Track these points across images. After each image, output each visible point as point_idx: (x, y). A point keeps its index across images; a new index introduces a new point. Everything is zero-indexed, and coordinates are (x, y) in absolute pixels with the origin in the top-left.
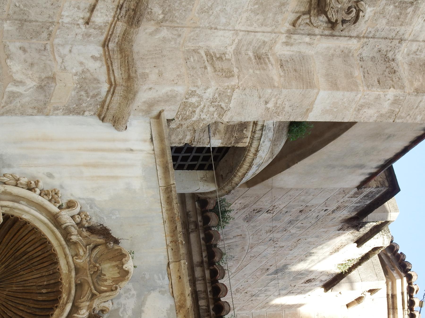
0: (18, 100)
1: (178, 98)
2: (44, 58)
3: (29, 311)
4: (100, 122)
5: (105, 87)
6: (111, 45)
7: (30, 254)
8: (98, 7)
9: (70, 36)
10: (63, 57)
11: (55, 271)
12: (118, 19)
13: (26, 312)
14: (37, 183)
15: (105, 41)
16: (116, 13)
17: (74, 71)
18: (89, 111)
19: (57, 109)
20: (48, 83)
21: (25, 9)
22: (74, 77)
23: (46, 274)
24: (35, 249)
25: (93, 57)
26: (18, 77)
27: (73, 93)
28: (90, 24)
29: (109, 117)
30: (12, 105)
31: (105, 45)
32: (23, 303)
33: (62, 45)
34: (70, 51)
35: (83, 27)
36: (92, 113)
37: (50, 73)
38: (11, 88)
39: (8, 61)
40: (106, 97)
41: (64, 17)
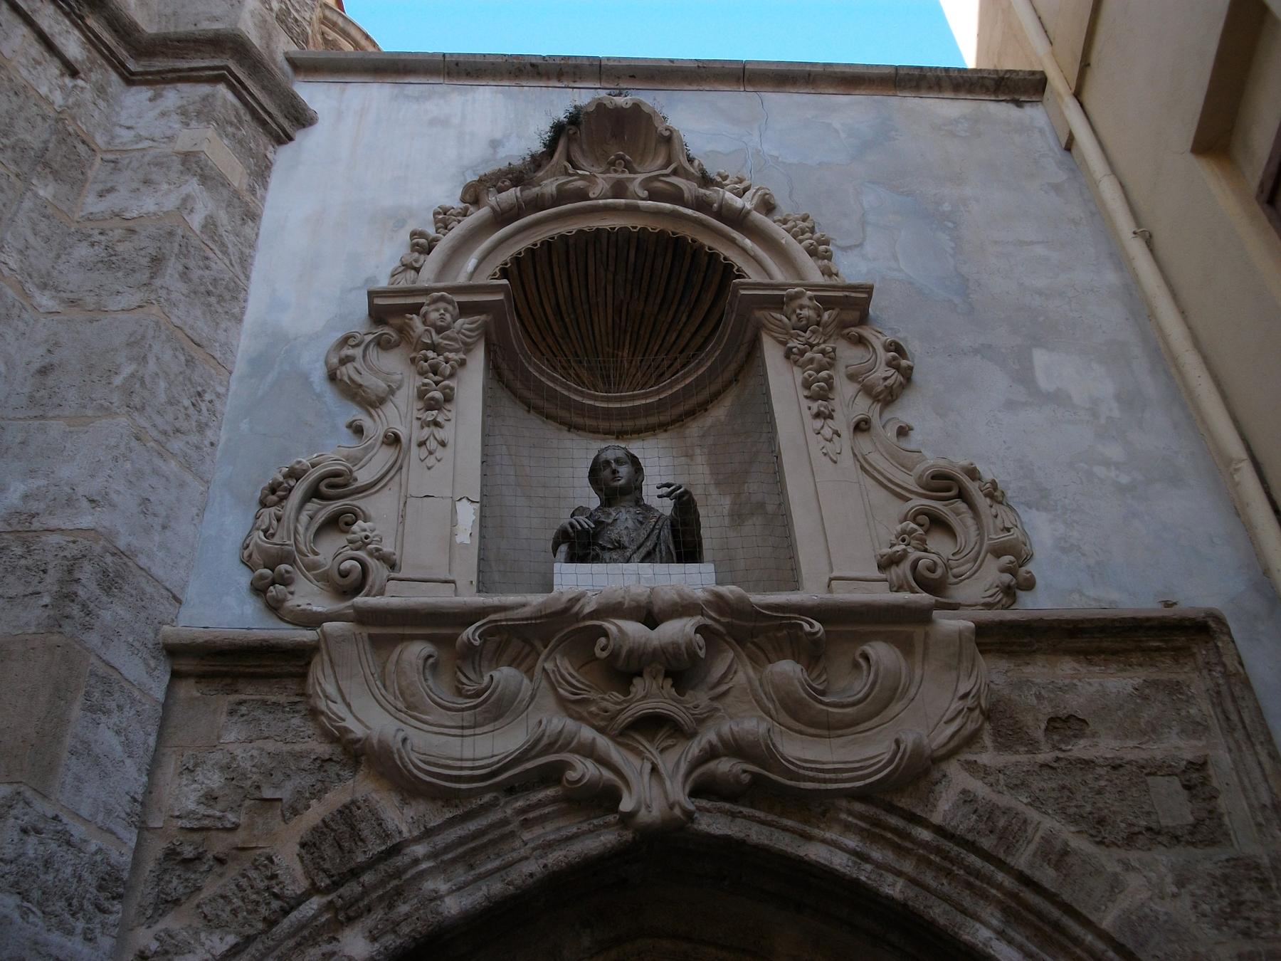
0: (221, 230)
1: (268, 19)
2: (135, 164)
3: (684, 318)
4: (291, 144)
5: (222, 89)
6: (132, 66)
7: (562, 301)
8: (46, 28)
9: (96, 114)
10: (139, 138)
11: (613, 238)
12: (82, 18)
13: (685, 323)
14: (421, 235)
15: (121, 75)
16: (67, 15)
17: (177, 126)
18: (266, 149)
19: (253, 191)
20: (196, 163)
21: (13, 139)
22: (192, 126)
23: (612, 268)
24: (554, 284)
25: (150, 100)
26: (171, 202)
27: (226, 141)
28: (78, 67)
29: (286, 124)
30: (230, 246)
31: (130, 79)
32: (663, 334)
33: (113, 138)
34: (129, 128)
35: (80, 82)
36: (271, 148)
37: (175, 158)
38: (196, 221)
39: (127, 215)
40: (246, 104)
41: (52, 98)
